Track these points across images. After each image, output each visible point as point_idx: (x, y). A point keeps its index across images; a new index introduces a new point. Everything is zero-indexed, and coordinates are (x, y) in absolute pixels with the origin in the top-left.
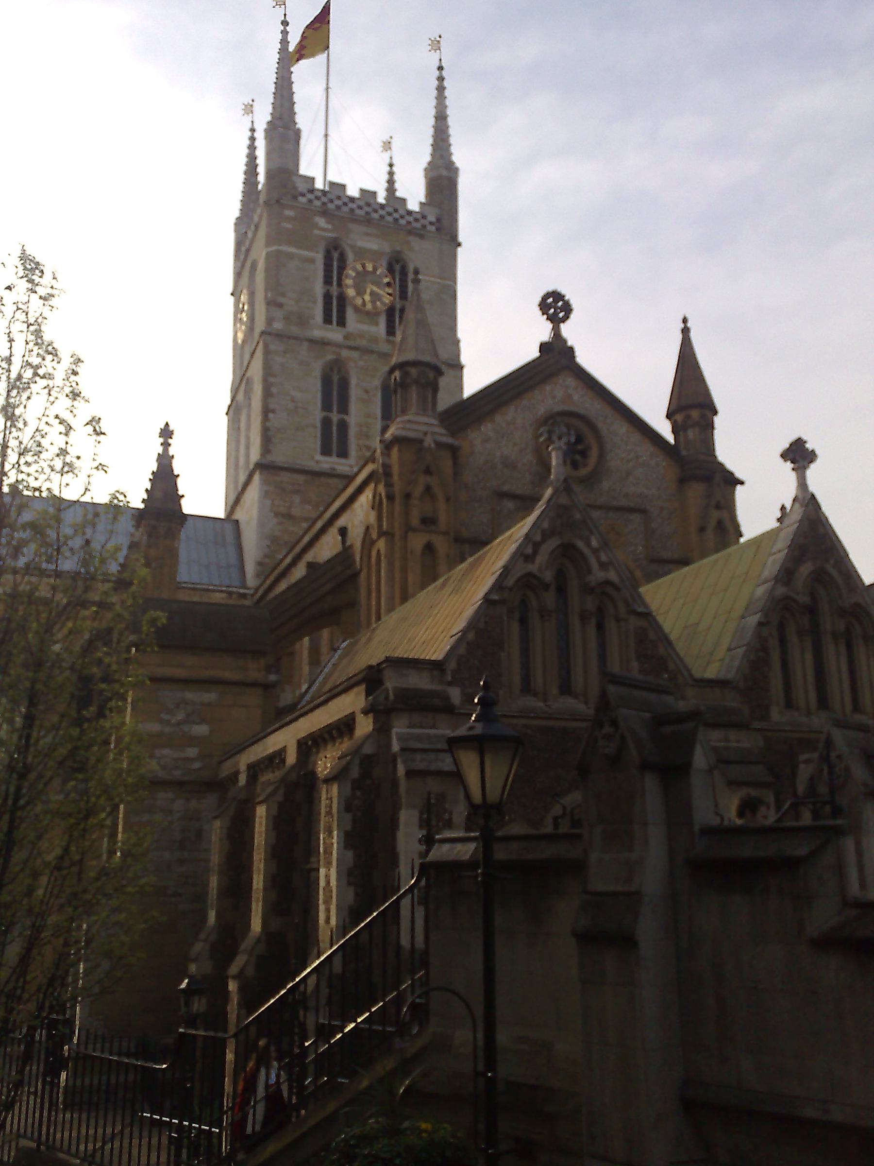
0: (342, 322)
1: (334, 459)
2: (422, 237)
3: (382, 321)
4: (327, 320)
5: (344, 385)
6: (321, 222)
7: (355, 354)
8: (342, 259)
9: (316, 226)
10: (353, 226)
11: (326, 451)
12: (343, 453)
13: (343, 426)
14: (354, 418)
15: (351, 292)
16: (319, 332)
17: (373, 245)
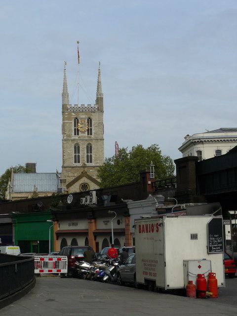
0: (78, 134)
1: (77, 163)
2: (94, 112)
3: (86, 133)
4: (75, 134)
5: (79, 147)
6: (73, 114)
7: (80, 141)
8: (78, 121)
9: (72, 115)
10: (80, 113)
11: (75, 162)
12: (79, 162)
13: (79, 156)
14: (81, 154)
15: (79, 128)
16: (74, 137)
17: (84, 117)
